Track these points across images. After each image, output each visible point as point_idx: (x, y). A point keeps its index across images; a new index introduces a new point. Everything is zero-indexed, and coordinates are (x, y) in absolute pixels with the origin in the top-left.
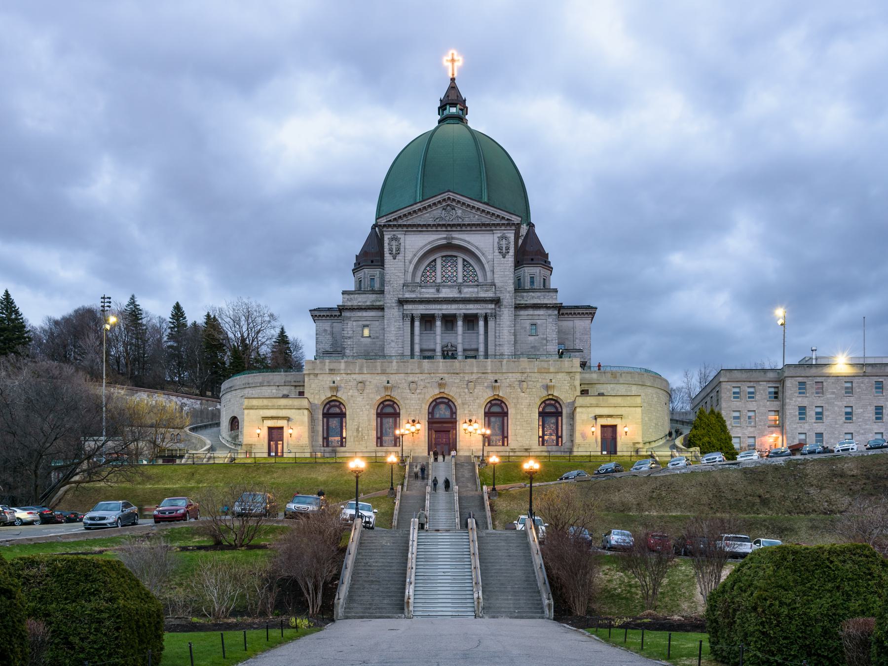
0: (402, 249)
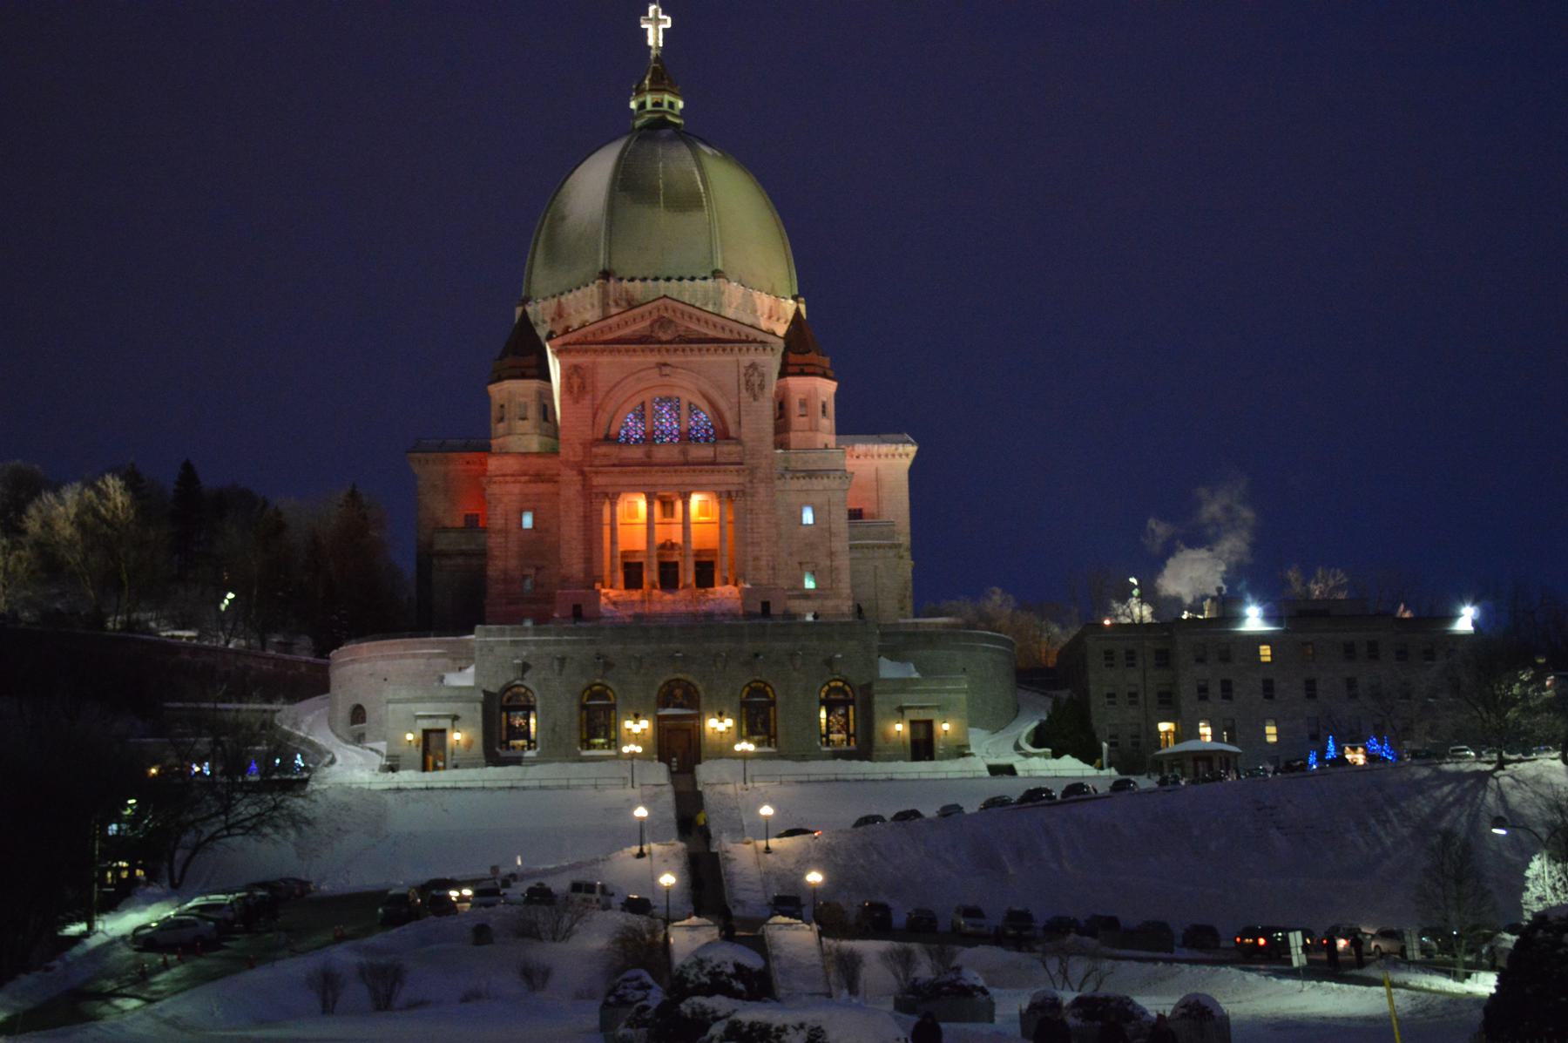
0: (589, 388)
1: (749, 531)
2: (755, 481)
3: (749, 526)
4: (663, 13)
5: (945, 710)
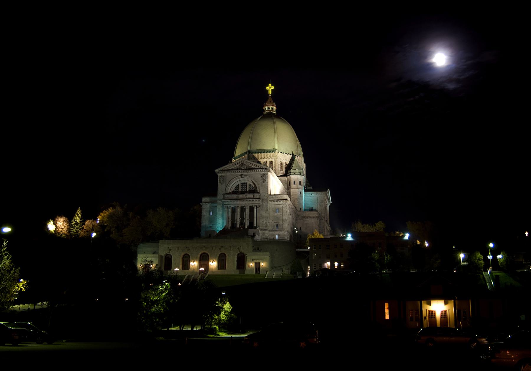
4: (272, 86)
5: (263, 260)
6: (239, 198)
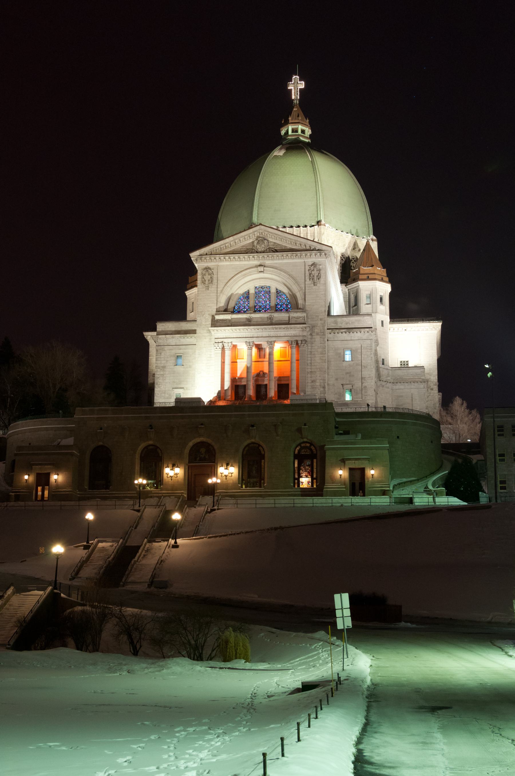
0: (215, 281)
1: (309, 364)
2: (313, 334)
3: (309, 362)
5: (373, 462)
6: (252, 323)
